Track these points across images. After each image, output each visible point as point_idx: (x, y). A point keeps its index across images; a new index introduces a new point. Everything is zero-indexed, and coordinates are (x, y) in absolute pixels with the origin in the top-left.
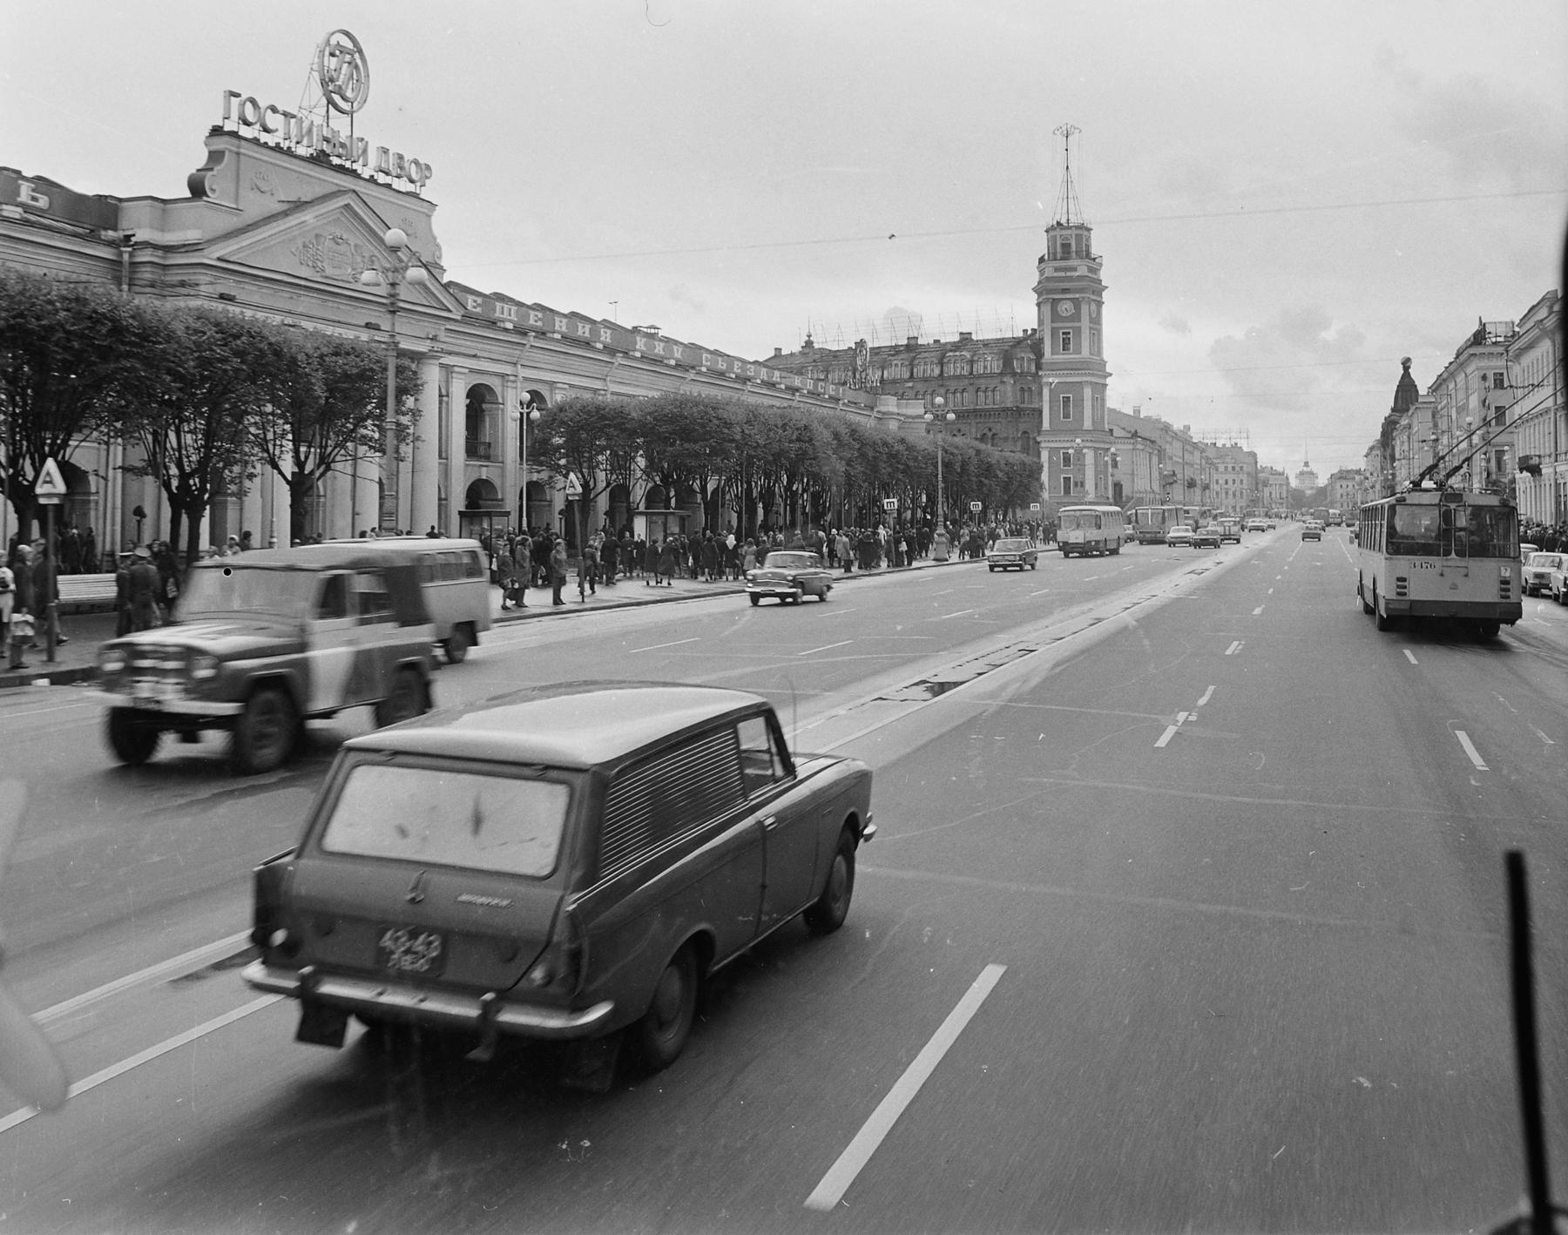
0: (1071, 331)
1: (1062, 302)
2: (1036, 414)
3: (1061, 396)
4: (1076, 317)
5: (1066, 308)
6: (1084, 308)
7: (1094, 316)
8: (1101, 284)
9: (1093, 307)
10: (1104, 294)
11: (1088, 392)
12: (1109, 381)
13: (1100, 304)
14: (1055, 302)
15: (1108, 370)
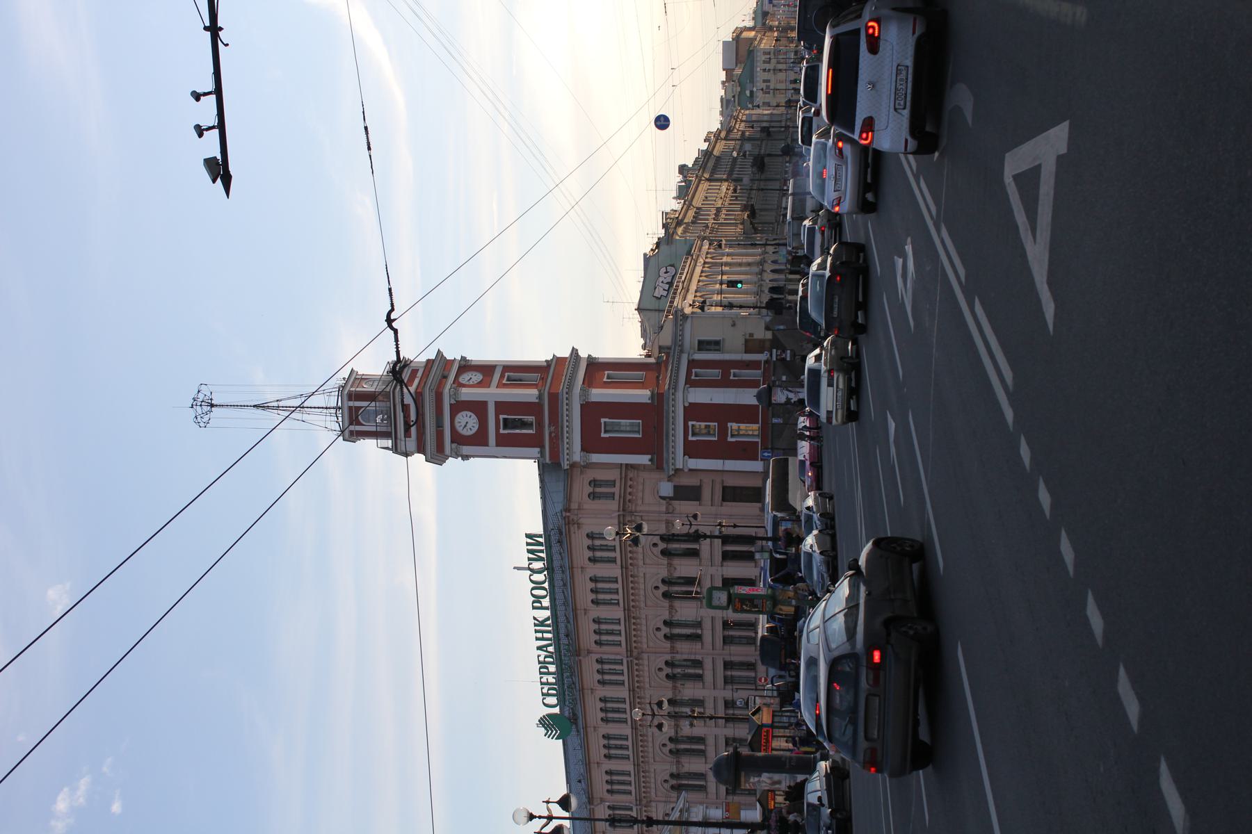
0: (501, 417)
1: (457, 425)
2: (631, 475)
3: (603, 435)
4: (478, 408)
5: (467, 423)
6: (467, 394)
7: (477, 377)
8: (433, 361)
9: (464, 378)
10: (449, 357)
11: (599, 394)
12: (583, 354)
13: (466, 366)
14: (458, 439)
15: (566, 353)
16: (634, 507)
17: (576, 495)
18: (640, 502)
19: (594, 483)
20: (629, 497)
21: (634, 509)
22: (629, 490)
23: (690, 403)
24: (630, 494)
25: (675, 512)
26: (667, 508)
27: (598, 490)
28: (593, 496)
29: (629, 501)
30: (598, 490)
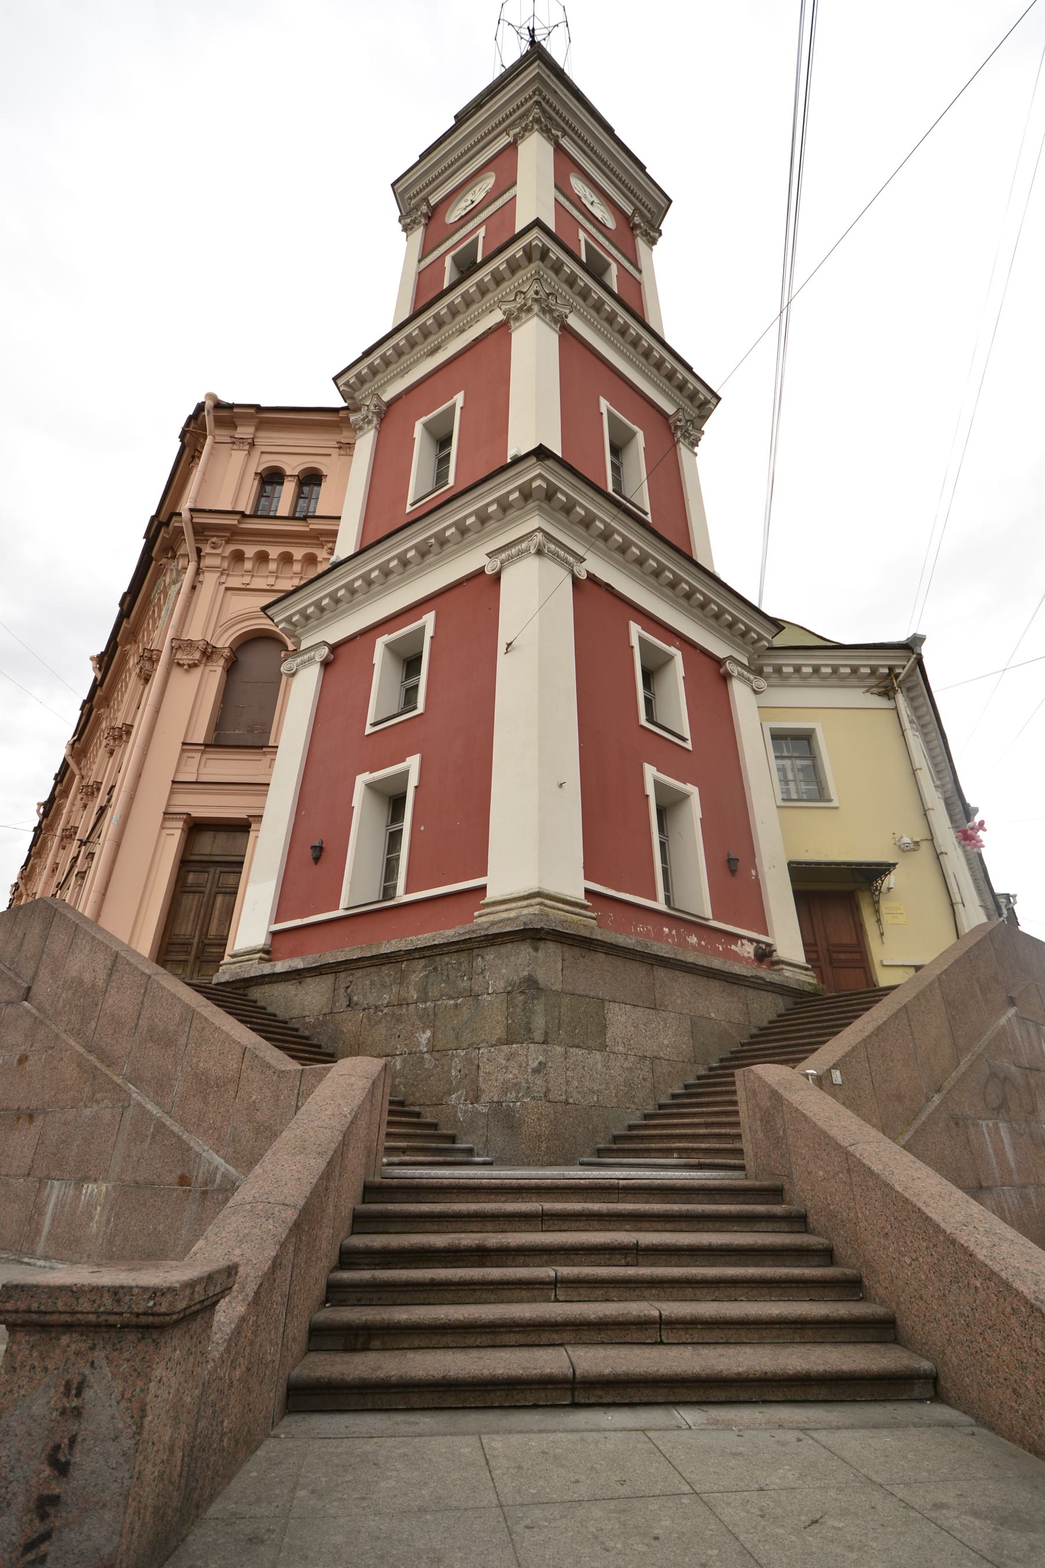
16: (216, 561)
17: (268, 439)
18: (234, 582)
19: (311, 479)
20: (250, 551)
21: (207, 562)
22: (274, 552)
23: (497, 578)
24: (262, 558)
25: (176, 672)
26: (190, 643)
27: (288, 489)
28: (272, 478)
29: (239, 557)
30: (288, 489)
